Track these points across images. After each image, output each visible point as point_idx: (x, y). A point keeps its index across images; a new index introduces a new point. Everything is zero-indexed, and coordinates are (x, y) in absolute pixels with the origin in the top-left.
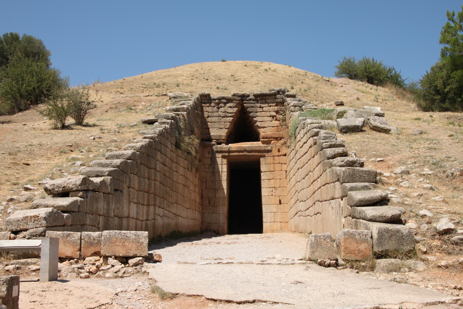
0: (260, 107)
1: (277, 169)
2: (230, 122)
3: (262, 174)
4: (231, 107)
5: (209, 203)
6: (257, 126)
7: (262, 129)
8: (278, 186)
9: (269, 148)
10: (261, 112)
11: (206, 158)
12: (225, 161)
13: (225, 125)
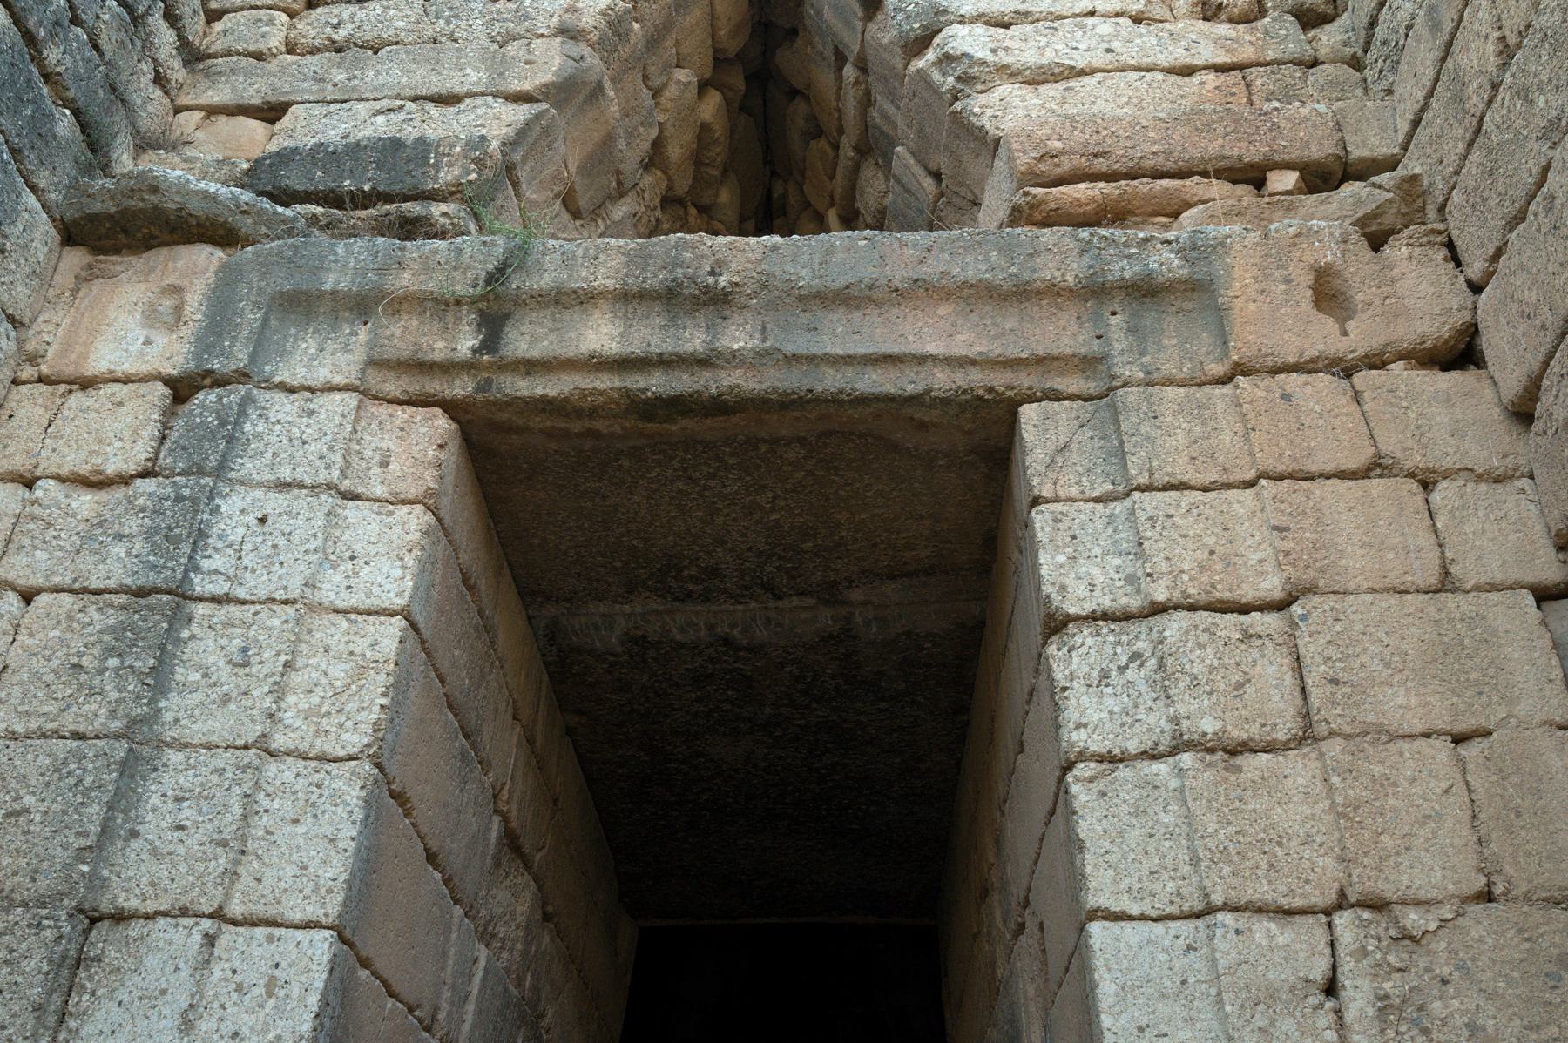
1: (1355, 563)
2: (568, 32)
3: (1075, 662)
6: (947, 59)
7: (1005, 89)
8: (1431, 867)
9: (1164, 262)
12: (417, 446)
13: (498, 64)
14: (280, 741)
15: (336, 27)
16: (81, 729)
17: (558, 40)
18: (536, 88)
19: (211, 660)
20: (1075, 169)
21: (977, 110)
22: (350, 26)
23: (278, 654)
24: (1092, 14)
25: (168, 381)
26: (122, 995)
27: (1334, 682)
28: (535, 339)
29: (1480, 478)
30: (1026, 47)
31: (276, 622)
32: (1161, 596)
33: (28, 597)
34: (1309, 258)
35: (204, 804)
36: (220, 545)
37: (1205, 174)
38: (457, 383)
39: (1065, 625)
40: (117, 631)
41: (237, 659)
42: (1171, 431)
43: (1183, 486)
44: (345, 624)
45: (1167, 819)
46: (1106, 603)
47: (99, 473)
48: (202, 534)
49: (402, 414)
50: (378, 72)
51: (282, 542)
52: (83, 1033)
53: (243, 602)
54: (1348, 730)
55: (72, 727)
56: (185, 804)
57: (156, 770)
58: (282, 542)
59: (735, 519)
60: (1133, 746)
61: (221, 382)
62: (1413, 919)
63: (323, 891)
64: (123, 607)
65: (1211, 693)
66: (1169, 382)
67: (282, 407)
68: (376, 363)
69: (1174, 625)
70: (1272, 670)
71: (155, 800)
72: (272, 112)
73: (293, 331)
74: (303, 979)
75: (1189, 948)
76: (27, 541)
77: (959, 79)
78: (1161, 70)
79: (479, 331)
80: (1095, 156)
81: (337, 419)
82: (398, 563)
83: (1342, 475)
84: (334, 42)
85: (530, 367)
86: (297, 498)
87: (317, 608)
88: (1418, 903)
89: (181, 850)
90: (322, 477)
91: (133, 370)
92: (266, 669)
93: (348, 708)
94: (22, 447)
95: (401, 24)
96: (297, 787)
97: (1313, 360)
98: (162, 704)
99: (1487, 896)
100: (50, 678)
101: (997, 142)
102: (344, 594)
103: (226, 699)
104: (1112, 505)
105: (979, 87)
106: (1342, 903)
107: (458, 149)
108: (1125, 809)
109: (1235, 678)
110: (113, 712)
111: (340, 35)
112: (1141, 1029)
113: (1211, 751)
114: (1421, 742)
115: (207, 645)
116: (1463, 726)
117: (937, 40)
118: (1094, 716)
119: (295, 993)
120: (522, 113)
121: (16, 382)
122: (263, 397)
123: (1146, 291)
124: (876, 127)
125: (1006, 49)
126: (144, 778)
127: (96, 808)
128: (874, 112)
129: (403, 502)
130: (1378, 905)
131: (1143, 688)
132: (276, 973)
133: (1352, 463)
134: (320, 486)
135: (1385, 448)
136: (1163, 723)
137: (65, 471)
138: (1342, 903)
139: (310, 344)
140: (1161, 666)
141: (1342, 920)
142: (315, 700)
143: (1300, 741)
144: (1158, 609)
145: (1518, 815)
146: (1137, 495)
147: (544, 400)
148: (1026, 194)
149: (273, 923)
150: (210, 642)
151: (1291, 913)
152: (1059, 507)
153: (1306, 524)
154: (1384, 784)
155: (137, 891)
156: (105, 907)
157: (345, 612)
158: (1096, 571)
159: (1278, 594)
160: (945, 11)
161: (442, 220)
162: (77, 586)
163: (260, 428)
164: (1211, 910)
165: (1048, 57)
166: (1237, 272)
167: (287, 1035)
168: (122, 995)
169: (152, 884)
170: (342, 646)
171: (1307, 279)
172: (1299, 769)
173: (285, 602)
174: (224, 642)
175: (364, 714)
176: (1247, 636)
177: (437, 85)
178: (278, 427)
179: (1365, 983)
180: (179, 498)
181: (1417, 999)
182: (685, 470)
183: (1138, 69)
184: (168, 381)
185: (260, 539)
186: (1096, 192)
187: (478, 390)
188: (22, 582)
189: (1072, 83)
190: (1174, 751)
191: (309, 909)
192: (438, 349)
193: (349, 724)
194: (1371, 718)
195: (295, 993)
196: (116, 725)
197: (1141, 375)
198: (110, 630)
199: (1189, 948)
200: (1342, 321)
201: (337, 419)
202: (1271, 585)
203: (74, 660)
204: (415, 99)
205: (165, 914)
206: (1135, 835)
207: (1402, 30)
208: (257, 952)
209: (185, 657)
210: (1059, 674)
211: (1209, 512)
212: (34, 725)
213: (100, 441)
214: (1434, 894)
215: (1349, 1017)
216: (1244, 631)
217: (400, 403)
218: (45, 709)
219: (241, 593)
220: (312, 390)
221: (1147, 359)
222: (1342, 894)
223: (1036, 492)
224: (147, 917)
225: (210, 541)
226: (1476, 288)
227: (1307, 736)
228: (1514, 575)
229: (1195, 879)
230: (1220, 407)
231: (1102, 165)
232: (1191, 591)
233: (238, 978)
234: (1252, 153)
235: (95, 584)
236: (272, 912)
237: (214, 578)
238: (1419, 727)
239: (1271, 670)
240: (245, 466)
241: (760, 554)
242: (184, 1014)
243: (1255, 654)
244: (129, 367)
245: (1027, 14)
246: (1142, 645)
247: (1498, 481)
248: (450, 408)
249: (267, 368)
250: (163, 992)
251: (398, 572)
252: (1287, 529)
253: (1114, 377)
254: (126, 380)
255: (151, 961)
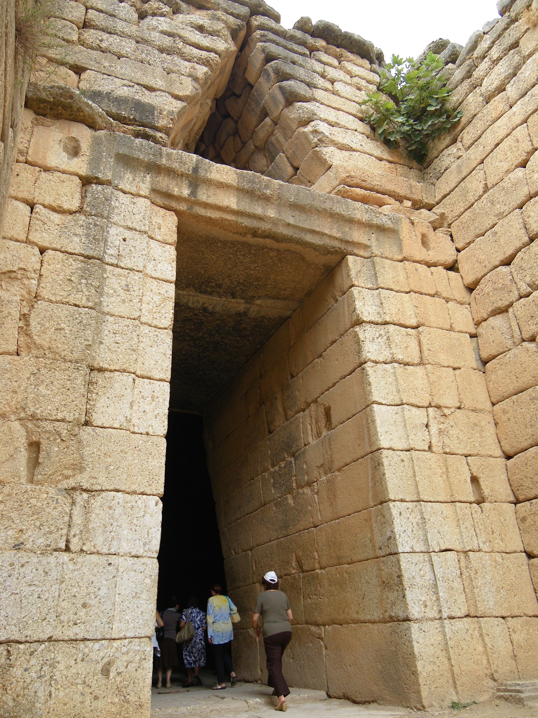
0: (323, 76)
1: (433, 320)
4: (201, 29)
5: (34, 463)
6: (315, 132)
7: (332, 149)
10: (326, 90)
11: (47, 170)
12: (167, 225)
14: (143, 319)
15: (101, 41)
16: (77, 303)
17: (190, 79)
18: (184, 96)
19: (116, 287)
20: (357, 183)
21: (324, 153)
22: (108, 43)
23: (139, 289)
24: (356, 130)
25: (81, 177)
26: (108, 395)
27: (429, 350)
28: (209, 197)
29: (458, 303)
30: (340, 136)
31: (137, 278)
32: (388, 320)
33: (42, 251)
34: (421, 231)
35: (124, 336)
36: (112, 245)
37: (389, 195)
38: (181, 205)
39: (362, 323)
40: (84, 270)
41: (125, 288)
42: (390, 273)
43: (392, 290)
44: (156, 283)
45: (390, 380)
46: (373, 319)
47: (61, 207)
48: (106, 241)
49: (162, 211)
50: (121, 68)
51: (133, 249)
52: (97, 405)
53: (123, 268)
54: (432, 363)
55: (73, 302)
56: (117, 335)
57: (104, 322)
58: (133, 249)
59: (239, 271)
60: (381, 360)
61: (99, 182)
62: (446, 411)
63: (164, 370)
64: (82, 262)
65: (400, 348)
66: (387, 258)
67: (124, 199)
68: (154, 191)
69: (391, 328)
70: (414, 344)
71: (106, 332)
72: (79, 70)
73: (122, 170)
74: (163, 396)
75: (396, 413)
76: (38, 228)
77: (318, 140)
78: (375, 157)
79: (190, 189)
80: (363, 181)
81: (144, 209)
82: (170, 265)
83: (429, 295)
84: (100, 47)
85: (206, 205)
86: (135, 234)
87: (146, 275)
88: (447, 407)
89: (119, 350)
90: (143, 228)
91: (66, 169)
92: (136, 293)
93: (162, 311)
94: (26, 189)
95: (128, 50)
96: (150, 335)
97: (421, 261)
98: (102, 299)
99: (459, 408)
100: (61, 282)
101: (330, 167)
102: (154, 272)
103: (124, 301)
104: (373, 291)
105: (324, 145)
106: (430, 406)
107: (165, 113)
108: (380, 376)
109: (405, 345)
110: (88, 299)
111: (104, 45)
112: (386, 432)
113: (400, 364)
114: (447, 368)
115: (114, 281)
116: (456, 366)
117: (312, 124)
118: (372, 350)
119: (161, 401)
120: (179, 105)
121: (18, 161)
122: (116, 192)
123: (381, 229)
124: (272, 143)
125: (334, 135)
126: (101, 324)
127: (89, 332)
128: (273, 139)
129: (167, 243)
130: (438, 407)
131: (383, 344)
132: (154, 394)
133: (432, 292)
134: (142, 231)
135: (439, 290)
136: (388, 354)
137: (46, 203)
138: (430, 406)
139: (129, 176)
140: (388, 339)
141: (430, 410)
142: (151, 307)
143: (419, 364)
144: (386, 323)
145: (466, 389)
146: (380, 290)
147: (210, 218)
148: (344, 187)
149: (150, 378)
150: (114, 280)
151: (419, 407)
152: (360, 289)
153: (422, 306)
154: (440, 377)
155: (106, 362)
156: (96, 365)
157: (155, 279)
158: (370, 309)
159: (415, 324)
160: (315, 114)
161: (160, 139)
162: (63, 249)
163: (117, 204)
164: (402, 404)
165: (345, 142)
166: (404, 230)
167: (160, 413)
168: (108, 395)
169: (111, 360)
170: (156, 290)
171: (420, 237)
172: (420, 370)
173: (138, 271)
174: (119, 281)
175: (167, 315)
176: (408, 335)
177: (145, 81)
178: (123, 206)
179: (435, 425)
180: (96, 225)
181: (447, 430)
182: (236, 251)
183: (369, 154)
184: (81, 177)
185: (125, 246)
186: (362, 192)
187: (188, 209)
188: (40, 243)
189: (351, 153)
190: (391, 362)
191: (161, 375)
192: (176, 191)
193: (163, 317)
194: (437, 361)
195: (161, 401)
196: (90, 304)
197: (380, 254)
198: (80, 269)
199: (396, 413)
200: (428, 251)
201: (144, 209)
202: (413, 322)
203: (69, 278)
204: (138, 84)
205: (118, 371)
206: (383, 383)
207: (443, 168)
208: (147, 387)
209: (106, 284)
210: (361, 337)
211: (398, 299)
212: (58, 299)
213: (58, 195)
214: (450, 406)
215: (432, 433)
216: (407, 333)
217: (161, 207)
218: (62, 294)
219: (122, 265)
220: (131, 194)
221: (381, 250)
222: (430, 404)
223: (354, 283)
224: (111, 371)
225: (108, 243)
226: (458, 251)
227: (421, 363)
228: (465, 330)
229: (398, 396)
230: (400, 269)
231: (364, 184)
232: (395, 320)
233: (142, 394)
234: (402, 193)
235: (70, 251)
236: (149, 375)
237: (112, 257)
238: (446, 365)
239: (413, 344)
240: (115, 218)
241: (239, 283)
242: (131, 403)
243: (409, 340)
244: (63, 167)
245: (339, 124)
246: (382, 332)
247: (461, 304)
248: (178, 213)
249: (116, 182)
250: (123, 396)
251: (170, 268)
252: (418, 307)
253: (373, 253)
254: (64, 172)
255: (116, 385)
